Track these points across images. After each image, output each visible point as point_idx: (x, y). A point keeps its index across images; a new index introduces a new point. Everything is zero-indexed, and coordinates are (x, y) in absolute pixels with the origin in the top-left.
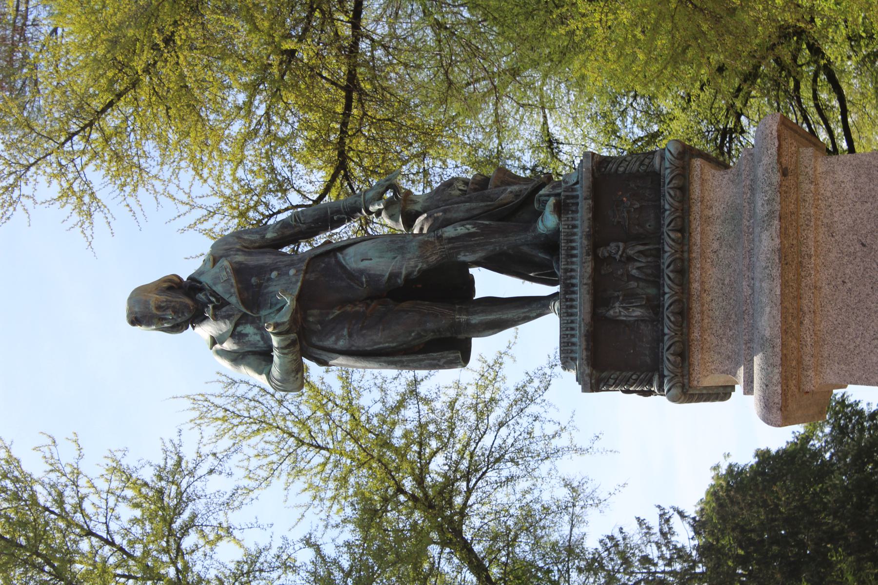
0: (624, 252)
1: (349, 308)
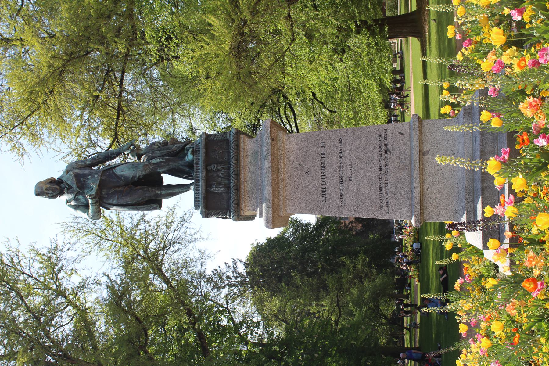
1: (117, 189)
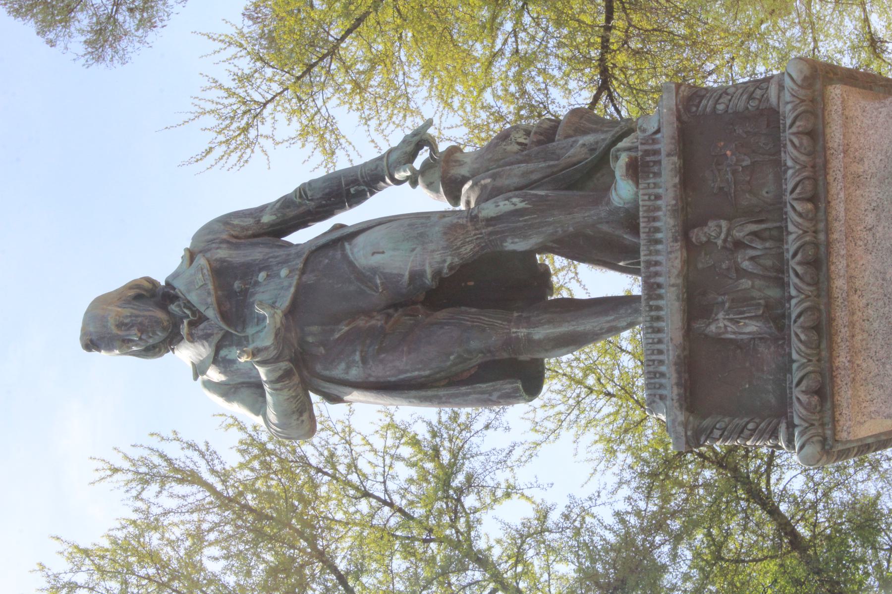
0: (728, 234)
1: (361, 322)
